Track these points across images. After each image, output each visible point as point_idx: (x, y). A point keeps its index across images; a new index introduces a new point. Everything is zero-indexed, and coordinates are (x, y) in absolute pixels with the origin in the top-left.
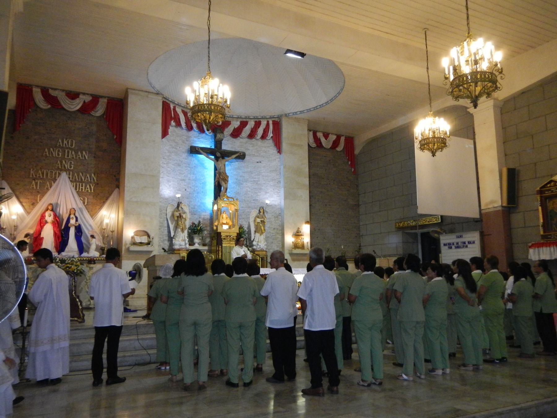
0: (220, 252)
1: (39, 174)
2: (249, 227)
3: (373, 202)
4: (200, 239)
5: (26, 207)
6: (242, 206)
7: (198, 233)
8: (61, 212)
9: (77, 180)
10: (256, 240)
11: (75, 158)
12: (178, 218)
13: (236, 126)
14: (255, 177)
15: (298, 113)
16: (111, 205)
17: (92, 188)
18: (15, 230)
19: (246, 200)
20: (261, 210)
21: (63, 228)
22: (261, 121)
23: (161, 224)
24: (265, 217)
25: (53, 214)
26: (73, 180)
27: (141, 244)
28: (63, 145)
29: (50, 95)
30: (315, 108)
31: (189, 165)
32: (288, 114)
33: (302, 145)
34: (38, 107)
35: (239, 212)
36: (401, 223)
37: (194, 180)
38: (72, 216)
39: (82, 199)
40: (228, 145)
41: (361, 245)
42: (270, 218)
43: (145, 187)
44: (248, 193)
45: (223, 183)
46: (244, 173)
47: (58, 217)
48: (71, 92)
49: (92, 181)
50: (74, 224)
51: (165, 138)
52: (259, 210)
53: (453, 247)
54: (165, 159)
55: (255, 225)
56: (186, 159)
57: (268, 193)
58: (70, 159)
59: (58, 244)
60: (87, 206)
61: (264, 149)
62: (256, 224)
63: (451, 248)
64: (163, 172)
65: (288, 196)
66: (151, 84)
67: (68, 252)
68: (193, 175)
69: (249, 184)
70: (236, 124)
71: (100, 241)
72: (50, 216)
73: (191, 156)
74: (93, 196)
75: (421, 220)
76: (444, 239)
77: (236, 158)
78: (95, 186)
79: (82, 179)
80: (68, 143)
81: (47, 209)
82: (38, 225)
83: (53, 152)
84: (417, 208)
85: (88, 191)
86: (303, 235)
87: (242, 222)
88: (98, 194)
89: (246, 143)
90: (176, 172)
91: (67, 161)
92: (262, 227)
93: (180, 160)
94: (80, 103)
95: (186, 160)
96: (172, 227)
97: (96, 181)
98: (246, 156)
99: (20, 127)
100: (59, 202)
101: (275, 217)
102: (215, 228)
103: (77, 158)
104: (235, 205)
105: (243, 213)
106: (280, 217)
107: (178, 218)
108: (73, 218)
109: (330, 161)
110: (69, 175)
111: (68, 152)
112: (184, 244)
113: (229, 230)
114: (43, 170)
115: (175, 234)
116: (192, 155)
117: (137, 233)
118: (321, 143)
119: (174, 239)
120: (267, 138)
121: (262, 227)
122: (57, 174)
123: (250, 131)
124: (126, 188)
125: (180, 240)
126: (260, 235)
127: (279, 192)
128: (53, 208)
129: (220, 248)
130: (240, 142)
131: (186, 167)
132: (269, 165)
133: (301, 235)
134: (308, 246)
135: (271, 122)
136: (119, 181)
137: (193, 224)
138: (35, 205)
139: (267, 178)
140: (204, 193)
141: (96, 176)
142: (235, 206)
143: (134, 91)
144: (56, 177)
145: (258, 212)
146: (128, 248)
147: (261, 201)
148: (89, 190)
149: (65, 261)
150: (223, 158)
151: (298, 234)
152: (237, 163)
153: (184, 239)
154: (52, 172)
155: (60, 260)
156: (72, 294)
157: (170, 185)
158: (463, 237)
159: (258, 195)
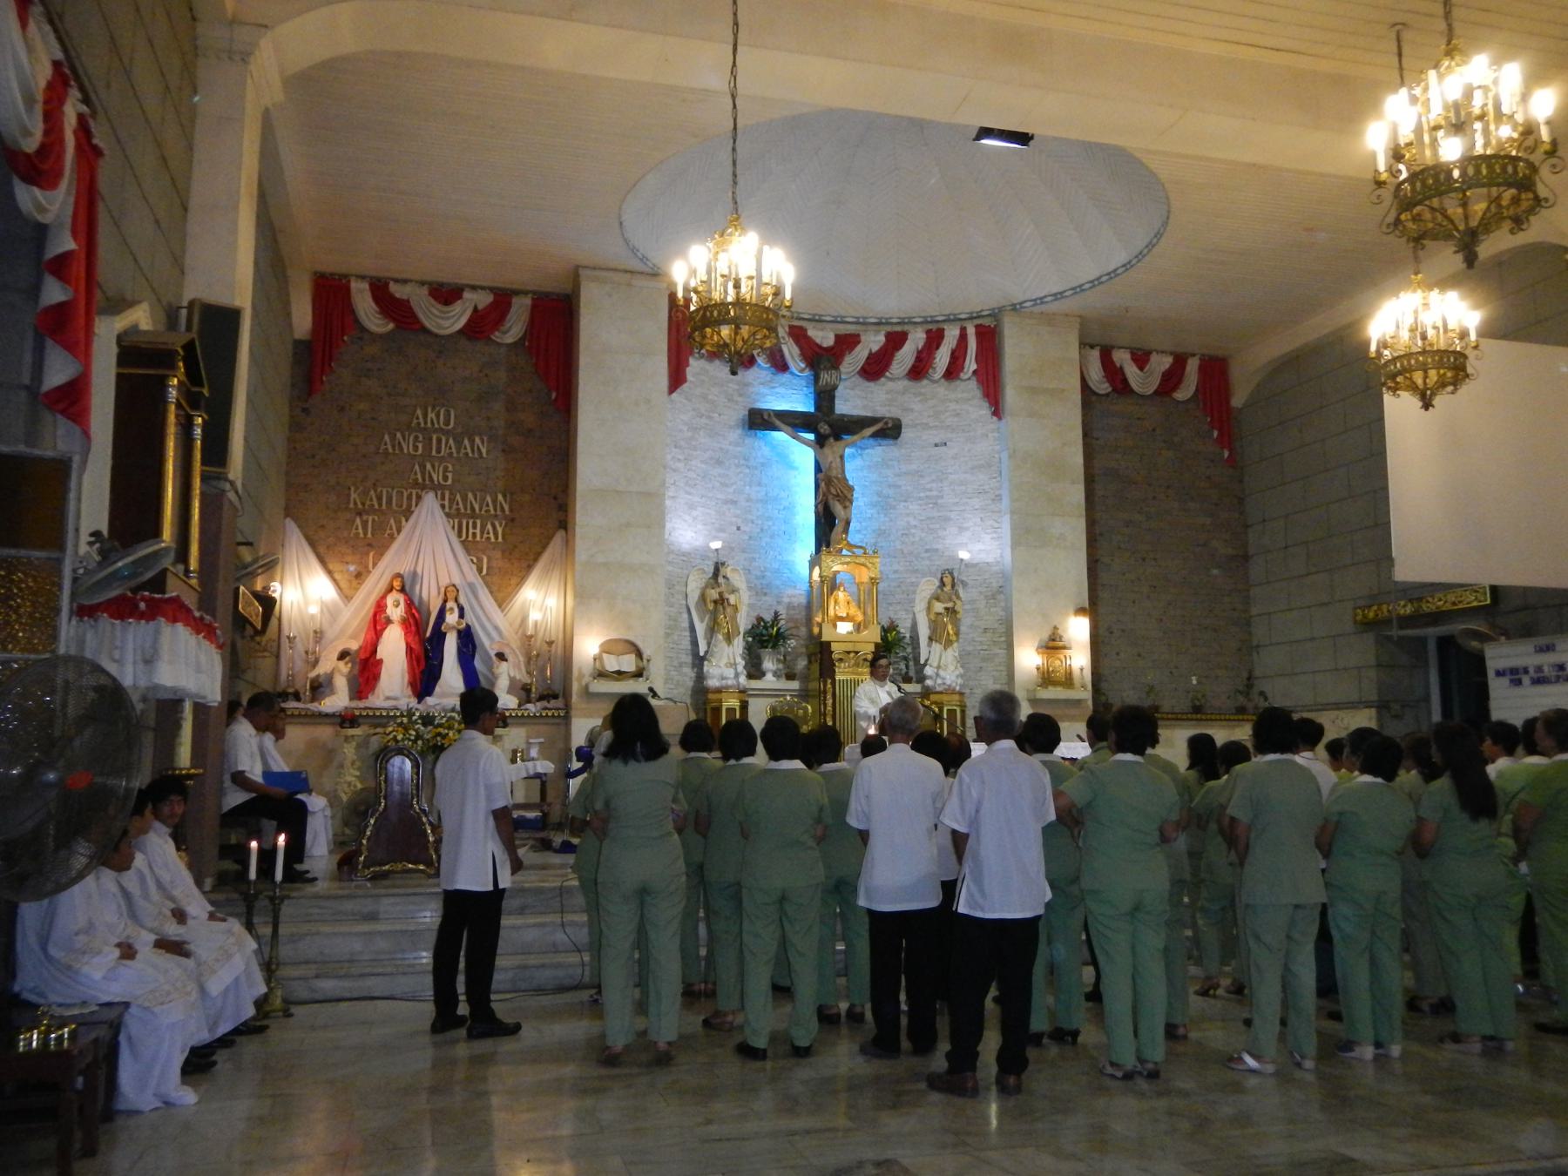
0: (829, 696)
1: (371, 500)
2: (914, 628)
3: (1286, 547)
4: (778, 660)
5: (344, 584)
6: (896, 567)
7: (770, 645)
8: (425, 595)
9: (463, 511)
10: (934, 661)
11: (455, 455)
12: (717, 606)
13: (875, 348)
14: (928, 486)
15: (1049, 299)
16: (547, 572)
17: (500, 530)
18: (317, 642)
19: (905, 551)
20: (945, 579)
21: (428, 634)
22: (944, 329)
23: (672, 623)
24: (958, 597)
25: (405, 601)
26: (453, 511)
27: (620, 675)
28: (426, 423)
29: (392, 297)
30: (1096, 283)
31: (745, 459)
32: (1021, 304)
33: (1063, 391)
34: (364, 330)
35: (880, 585)
36: (1370, 607)
37: (761, 501)
38: (451, 604)
39: (475, 560)
40: (852, 400)
41: (1257, 673)
42: (973, 602)
43: (628, 525)
44: (913, 531)
45: (837, 508)
46: (899, 475)
47: (416, 608)
48: (442, 285)
49: (499, 513)
50: (455, 624)
51: (678, 390)
52: (942, 579)
53: (1526, 680)
54: (680, 447)
55: (930, 620)
56: (737, 445)
57: (967, 529)
58: (442, 459)
59: (418, 676)
60: (488, 578)
61: (953, 406)
62: (932, 617)
63: (1518, 683)
65: (1026, 535)
66: (634, 251)
67: (444, 695)
68: (758, 488)
69: (914, 507)
70: (873, 341)
71: (520, 669)
72: (397, 606)
73: (750, 436)
74: (503, 552)
75: (1430, 599)
76: (1499, 656)
77: (875, 435)
78: (506, 526)
79: (473, 509)
80: (438, 416)
81: (390, 589)
82: (368, 629)
83: (402, 441)
84: (1393, 566)
85: (488, 538)
86: (1070, 648)
87: (896, 612)
88: (515, 547)
89: (904, 394)
90: (710, 479)
91: (437, 464)
92: (950, 627)
93: (721, 449)
94: (465, 311)
95: (739, 449)
96: (700, 628)
97: (507, 513)
98: (903, 430)
99: (322, 382)
100: (419, 571)
101: (986, 596)
102: (816, 630)
103: (461, 455)
104: (870, 565)
105: (899, 586)
106: (1002, 596)
107: (717, 606)
108: (452, 609)
109: (1154, 430)
110: (443, 498)
111: (439, 441)
112: (732, 676)
113: (856, 637)
114: (379, 490)
115: (709, 647)
116: (756, 435)
117: (608, 648)
118: (1125, 381)
119: (706, 663)
120: (962, 375)
121: (950, 627)
122: (414, 497)
123: (913, 359)
124: (578, 530)
125: (725, 661)
126: (945, 649)
127: (996, 525)
128: (404, 585)
129: (829, 686)
131: (737, 466)
132: (969, 451)
133: (1064, 648)
134: (1082, 677)
135: (971, 331)
136: (566, 511)
137: (760, 619)
138: (363, 577)
139: (964, 488)
140: (790, 535)
141: (508, 499)
142: (868, 568)
143: (597, 273)
144: (410, 506)
145: (937, 583)
146: (587, 687)
147: (946, 554)
148: (492, 535)
149: (434, 717)
150: (838, 438)
151: (1053, 645)
153: (732, 661)
154: (402, 493)
155: (421, 717)
156: (412, 805)
157: (695, 518)
158: (1558, 648)
159: (939, 537)
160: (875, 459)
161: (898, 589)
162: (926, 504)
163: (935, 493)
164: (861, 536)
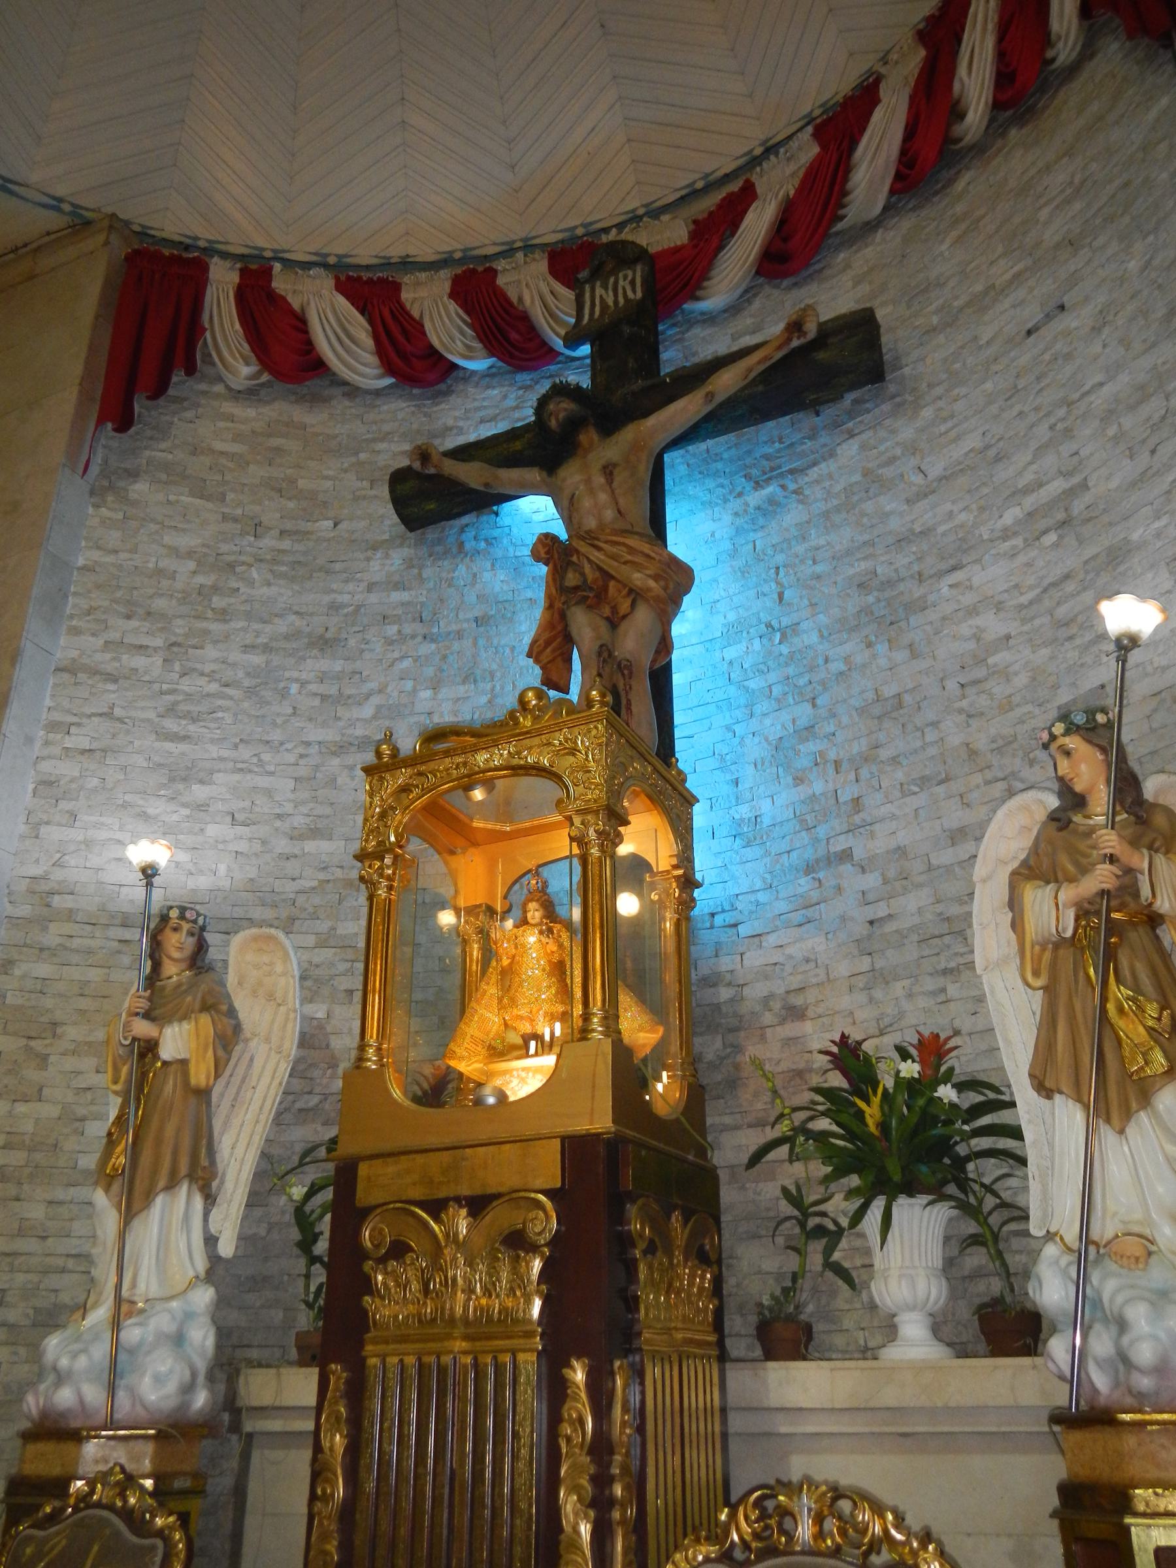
14: (1029, 477)
19: (981, 743)
56: (398, 586)
64: (108, 715)
68: (461, 690)
90: (284, 694)
93: (334, 607)
95: (397, 596)
116: (461, 545)
130: (857, 282)
145: (1053, 802)
152: (849, 450)
160: (838, 488)
162: (1028, 544)
163: (1058, 486)
164: (812, 747)
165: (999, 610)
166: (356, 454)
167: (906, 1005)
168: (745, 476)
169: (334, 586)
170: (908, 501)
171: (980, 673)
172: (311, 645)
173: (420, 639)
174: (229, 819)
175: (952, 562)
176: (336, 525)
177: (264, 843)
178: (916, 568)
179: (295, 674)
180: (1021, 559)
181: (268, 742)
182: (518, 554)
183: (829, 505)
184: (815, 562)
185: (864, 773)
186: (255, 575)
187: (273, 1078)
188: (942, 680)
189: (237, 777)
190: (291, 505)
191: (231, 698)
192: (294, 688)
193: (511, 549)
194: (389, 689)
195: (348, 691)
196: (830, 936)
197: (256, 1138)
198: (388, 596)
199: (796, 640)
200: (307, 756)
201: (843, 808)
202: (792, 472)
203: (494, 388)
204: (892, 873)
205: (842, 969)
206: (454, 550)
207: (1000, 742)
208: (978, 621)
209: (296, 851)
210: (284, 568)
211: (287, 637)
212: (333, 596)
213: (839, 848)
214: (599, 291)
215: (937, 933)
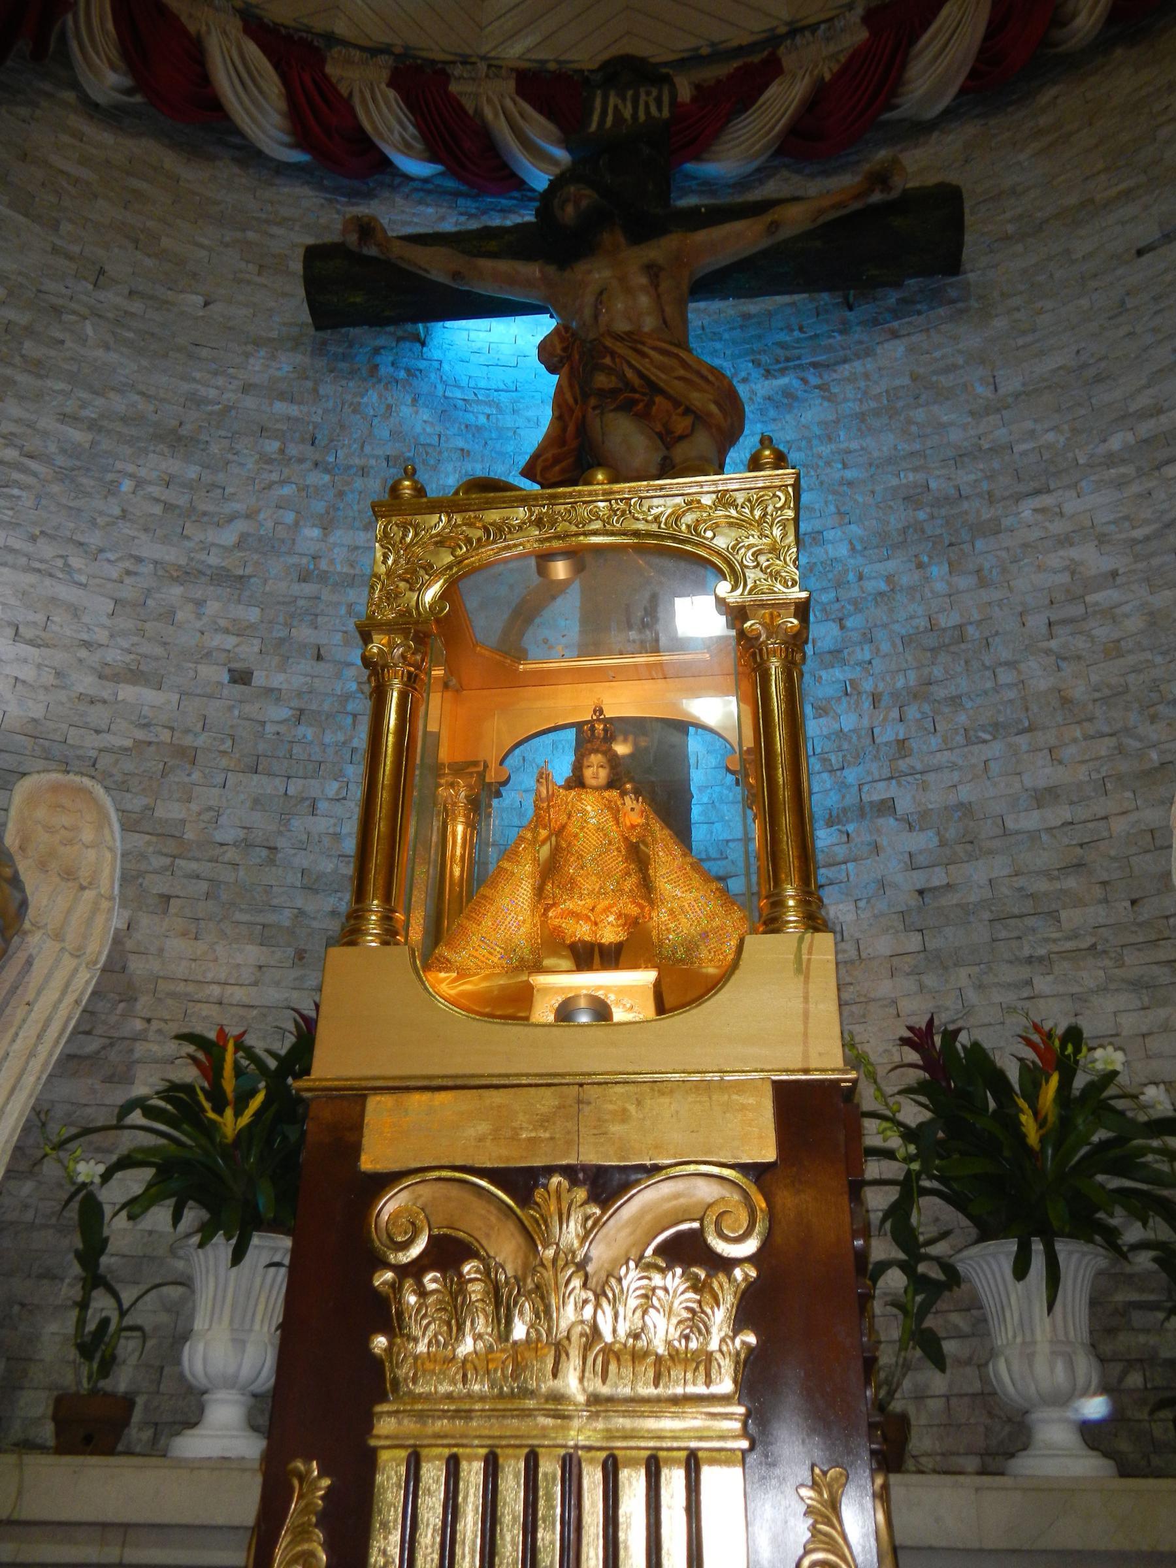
6: (1042, 774)
19: (1079, 691)
56: (282, 396)
73: (353, 373)
90: (111, 490)
93: (194, 400)
95: (280, 407)
160: (876, 390)
161: (1071, 883)
162: (1141, 473)
164: (838, 674)
165: (1101, 542)
166: (244, 230)
167: (972, 996)
168: (753, 362)
169: (198, 375)
170: (972, 413)
171: (1076, 610)
172: (157, 437)
173: (308, 465)
174: (10, 632)
175: (1034, 485)
176: (206, 304)
177: (58, 674)
178: (985, 486)
179: (131, 468)
180: (1135, 488)
181: (81, 544)
182: (448, 394)
183: (865, 407)
184: (845, 466)
185: (912, 712)
186: (89, 330)
187: (64, 992)
188: (1021, 614)
189: (31, 578)
190: (149, 262)
191: (35, 475)
192: (127, 485)
193: (440, 387)
194: (262, 516)
195: (202, 507)
196: (862, 904)
197: (29, 1080)
198: (271, 405)
199: (818, 551)
200: (136, 574)
201: (884, 749)
202: (815, 365)
203: (428, 205)
204: (951, 834)
205: (883, 945)
206: (364, 372)
207: (1107, 692)
208: (1074, 553)
209: (105, 695)
210: (131, 335)
211: (124, 420)
212: (194, 386)
213: (876, 797)
214: (613, 100)
215: (1016, 911)
